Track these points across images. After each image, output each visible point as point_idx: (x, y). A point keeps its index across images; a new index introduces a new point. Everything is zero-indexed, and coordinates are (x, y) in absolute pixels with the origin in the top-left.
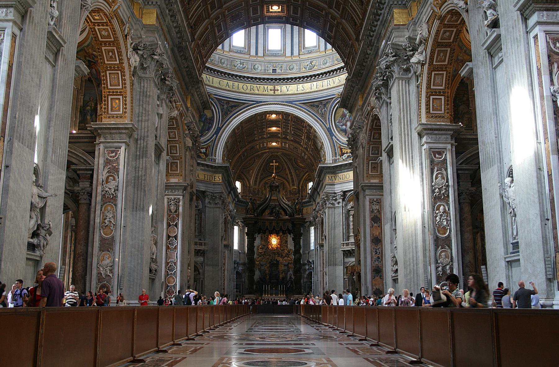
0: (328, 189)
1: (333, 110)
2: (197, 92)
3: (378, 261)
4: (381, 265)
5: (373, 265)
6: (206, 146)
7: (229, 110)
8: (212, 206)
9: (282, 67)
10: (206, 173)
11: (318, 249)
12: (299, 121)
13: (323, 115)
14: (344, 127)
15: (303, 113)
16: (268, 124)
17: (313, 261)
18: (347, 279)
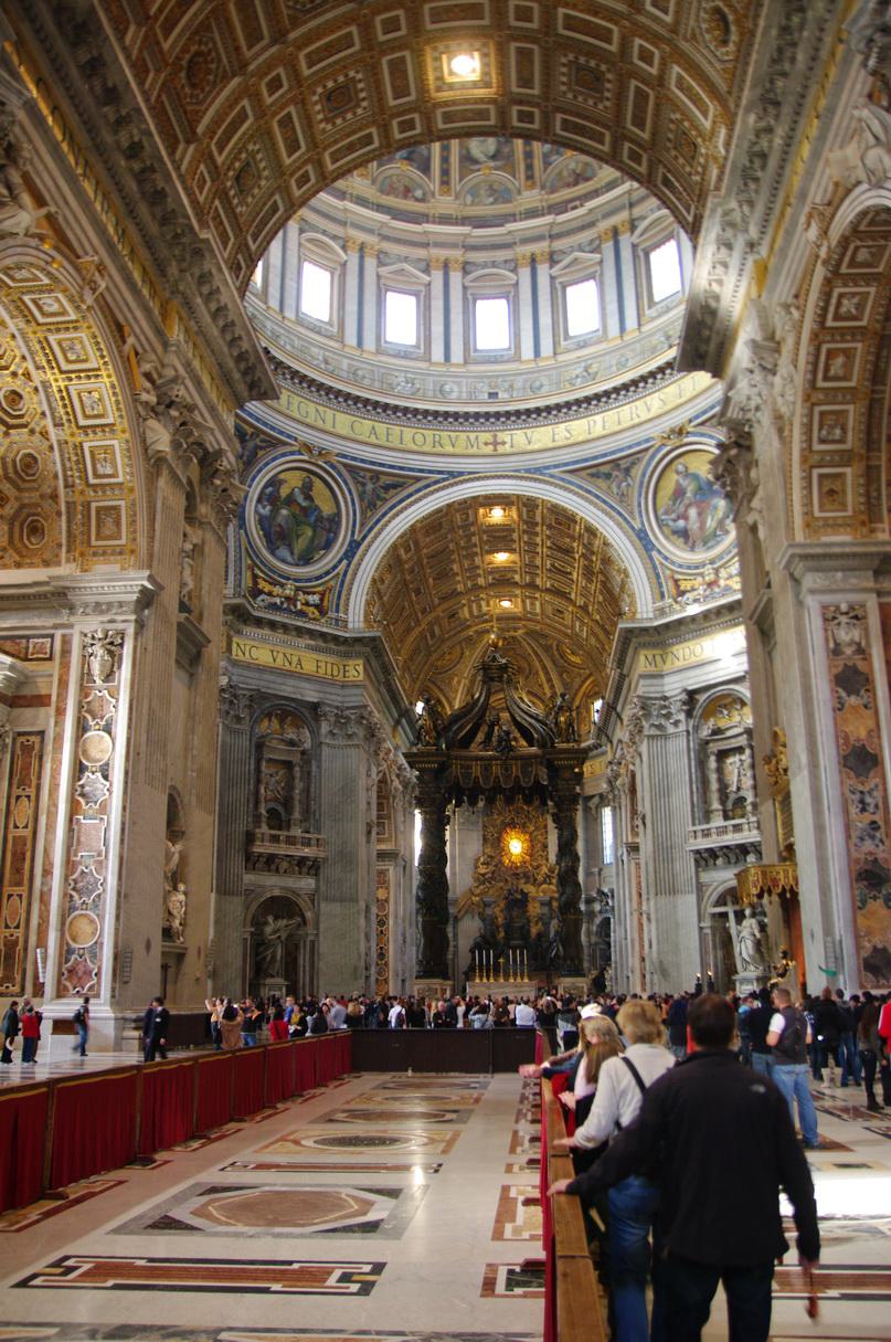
0: (643, 688)
1: (649, 482)
2: (208, 299)
3: (873, 838)
4: (885, 855)
5: (855, 855)
6: (320, 589)
7: (379, 497)
8: (341, 742)
9: (511, 386)
10: (322, 657)
11: (625, 858)
12: (562, 519)
13: (622, 497)
14: (681, 523)
15: (570, 495)
16: (486, 543)
17: (612, 891)
18: (708, 931)
